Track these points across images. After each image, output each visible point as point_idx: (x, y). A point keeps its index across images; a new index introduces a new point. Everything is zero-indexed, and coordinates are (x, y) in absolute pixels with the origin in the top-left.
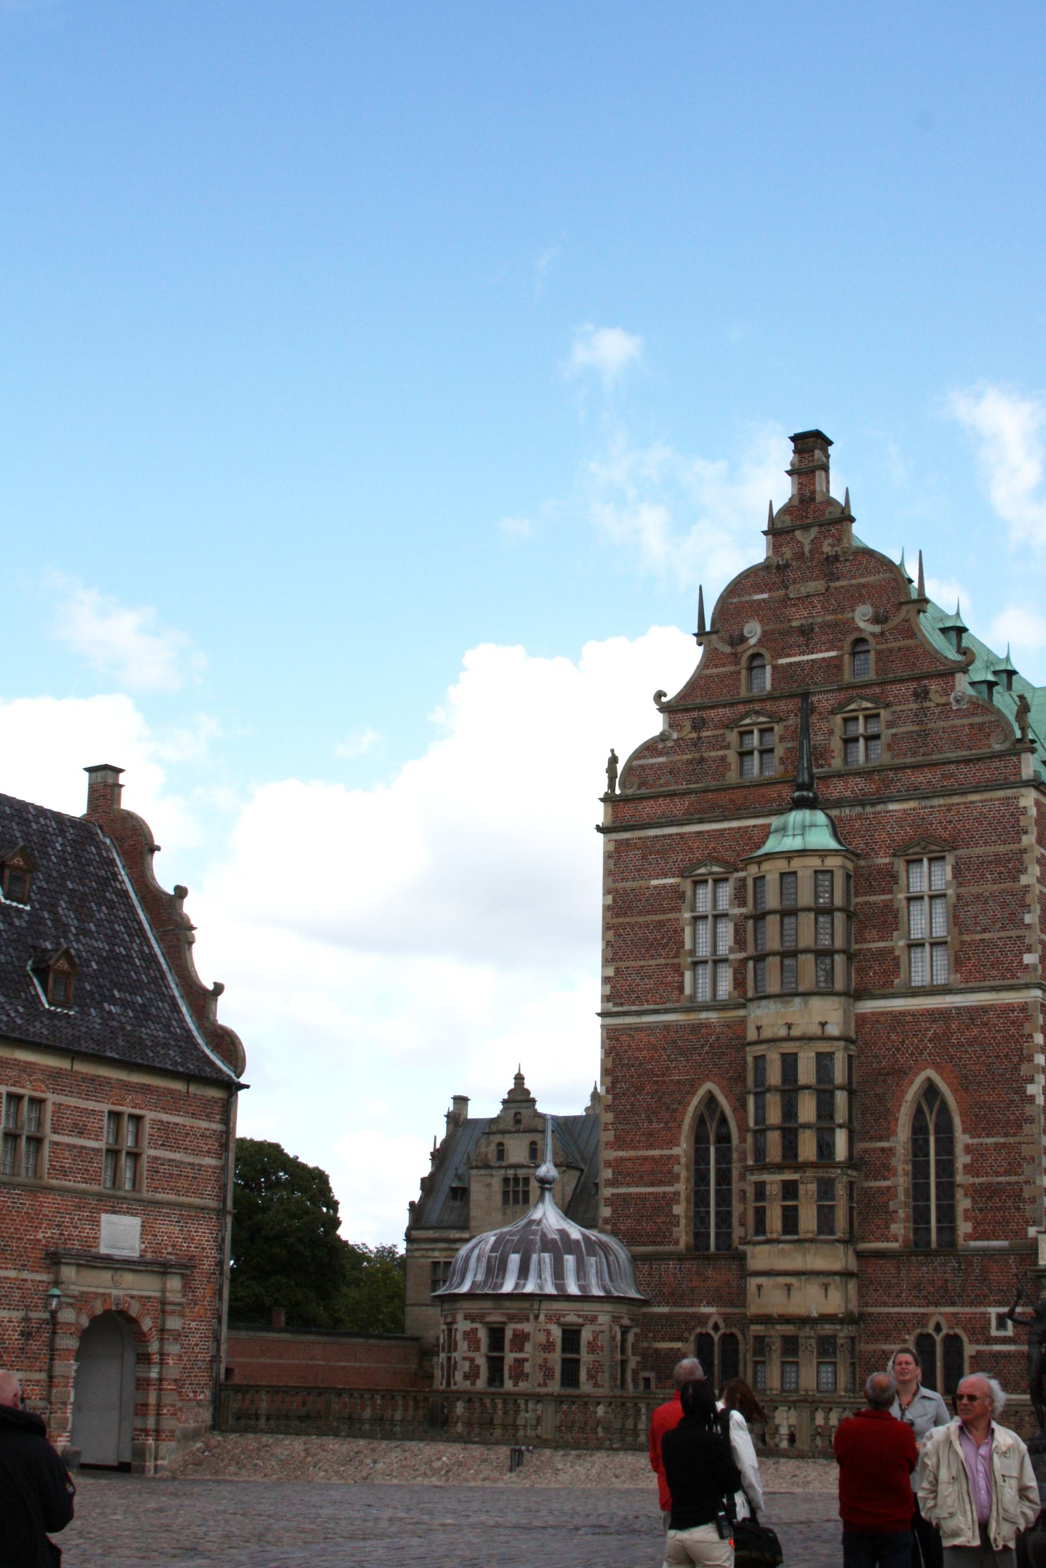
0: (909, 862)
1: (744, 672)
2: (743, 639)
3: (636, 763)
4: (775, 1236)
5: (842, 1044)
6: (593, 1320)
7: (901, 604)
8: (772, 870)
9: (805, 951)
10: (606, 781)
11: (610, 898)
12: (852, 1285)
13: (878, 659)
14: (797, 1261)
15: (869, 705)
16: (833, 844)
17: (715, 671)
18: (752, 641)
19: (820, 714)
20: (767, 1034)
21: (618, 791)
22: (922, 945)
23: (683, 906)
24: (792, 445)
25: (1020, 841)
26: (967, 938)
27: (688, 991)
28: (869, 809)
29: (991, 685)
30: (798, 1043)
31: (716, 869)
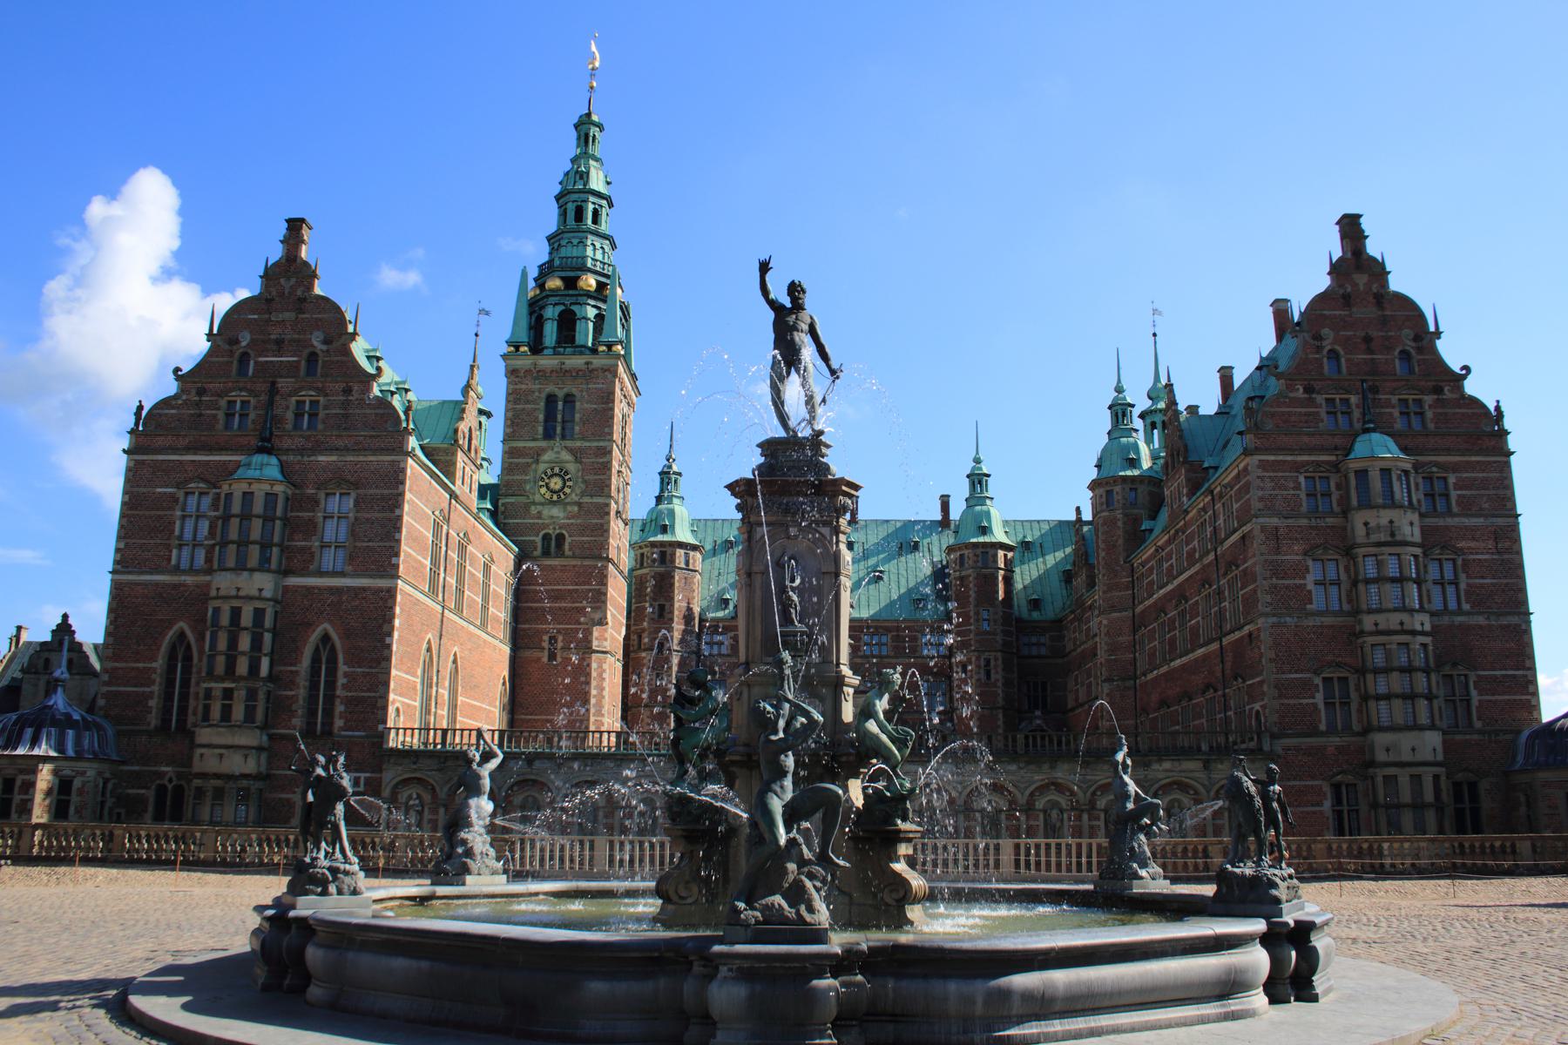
0: (327, 495)
1: (235, 362)
2: (237, 342)
3: (155, 411)
4: (215, 722)
5: (272, 603)
6: (84, 773)
10: (134, 421)
11: (127, 496)
12: (264, 756)
14: (229, 740)
15: (313, 393)
17: (217, 359)
18: (244, 344)
19: (282, 395)
20: (222, 593)
21: (141, 428)
22: (330, 547)
23: (177, 507)
24: (286, 225)
26: (359, 544)
27: (174, 562)
28: (306, 459)
29: (393, 393)
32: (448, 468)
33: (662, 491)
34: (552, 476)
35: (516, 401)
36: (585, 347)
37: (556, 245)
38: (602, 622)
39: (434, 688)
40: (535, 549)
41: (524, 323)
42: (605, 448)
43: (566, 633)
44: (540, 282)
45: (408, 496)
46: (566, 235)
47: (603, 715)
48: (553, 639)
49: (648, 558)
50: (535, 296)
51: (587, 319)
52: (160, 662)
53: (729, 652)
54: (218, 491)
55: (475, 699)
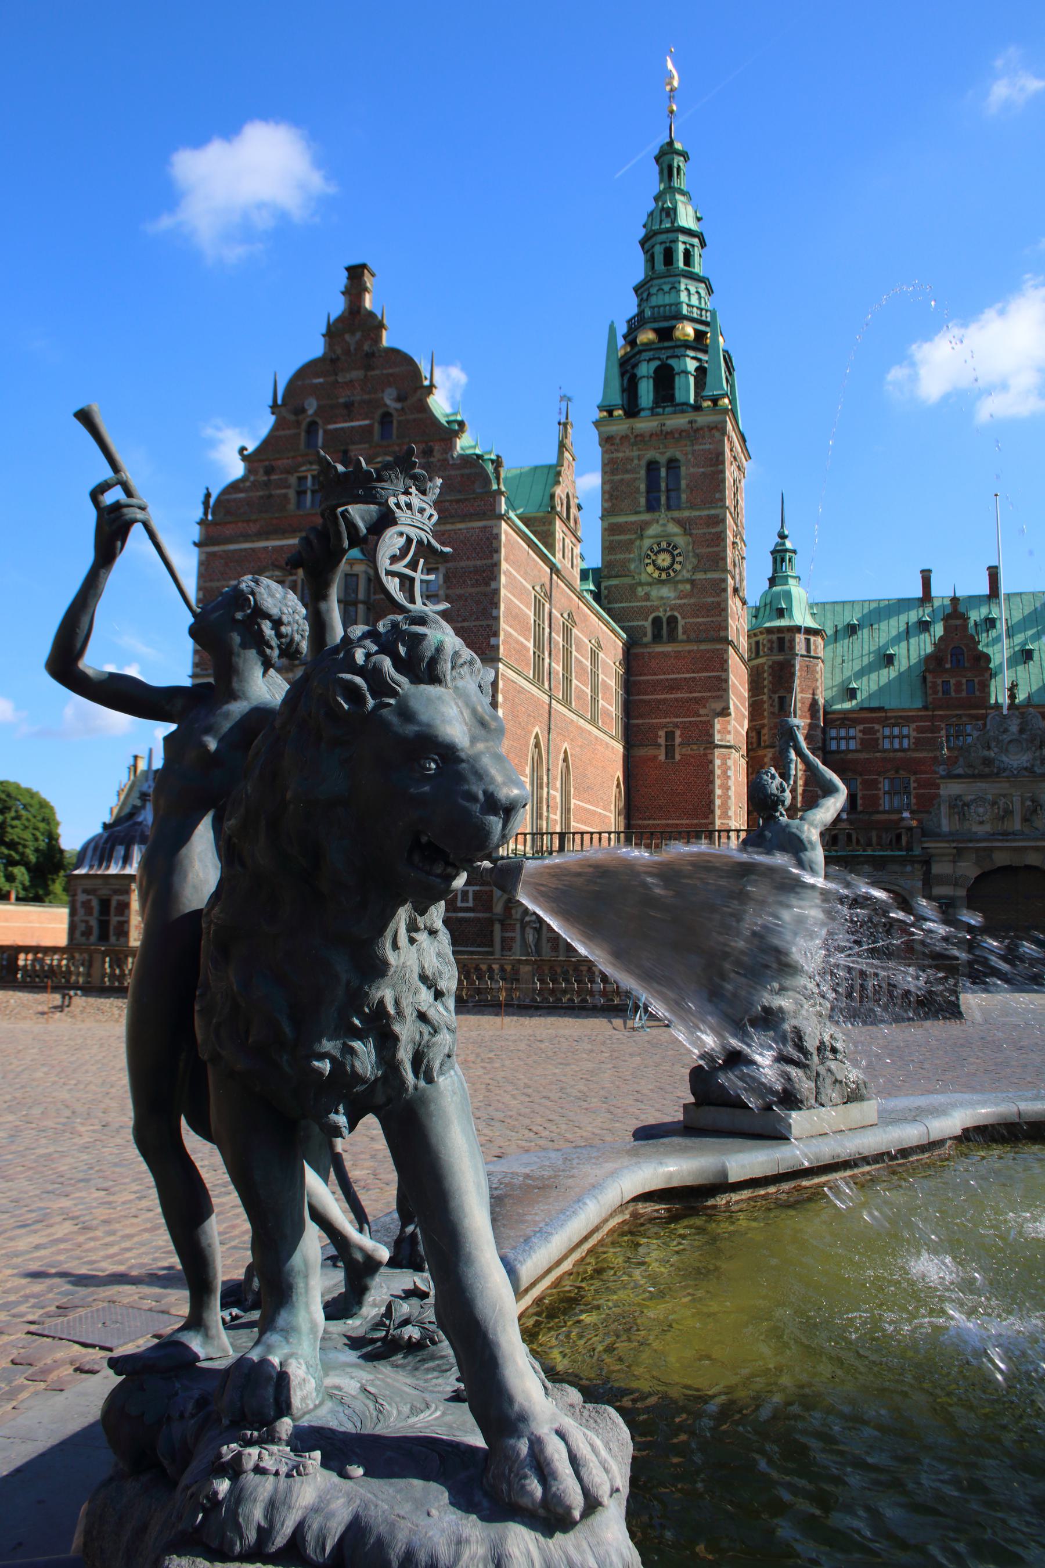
1: (303, 434)
2: (303, 410)
11: (201, 593)
18: (310, 412)
21: (210, 517)
24: (346, 274)
25: (492, 557)
32: (547, 538)
33: (775, 571)
34: (659, 552)
35: (613, 472)
36: (687, 404)
37: (645, 295)
38: (725, 712)
39: (545, 790)
40: (645, 635)
41: (616, 384)
42: (717, 516)
43: (684, 727)
44: (630, 338)
45: (504, 566)
46: (656, 282)
47: (729, 818)
48: (670, 736)
49: (764, 646)
50: (626, 354)
51: (686, 372)
53: (859, 747)
54: (294, 578)
55: (589, 802)
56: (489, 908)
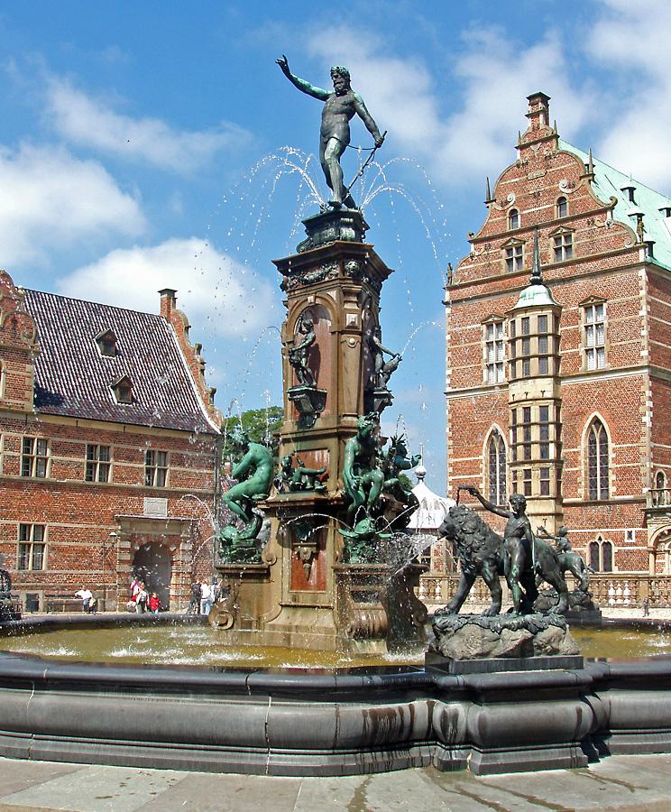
2: (507, 202)
7: (581, 177)
8: (518, 319)
9: (534, 356)
13: (570, 207)
16: (549, 302)
18: (511, 204)
27: (485, 379)
30: (531, 402)
31: (496, 319)
52: (484, 454)
56: (645, 543)
